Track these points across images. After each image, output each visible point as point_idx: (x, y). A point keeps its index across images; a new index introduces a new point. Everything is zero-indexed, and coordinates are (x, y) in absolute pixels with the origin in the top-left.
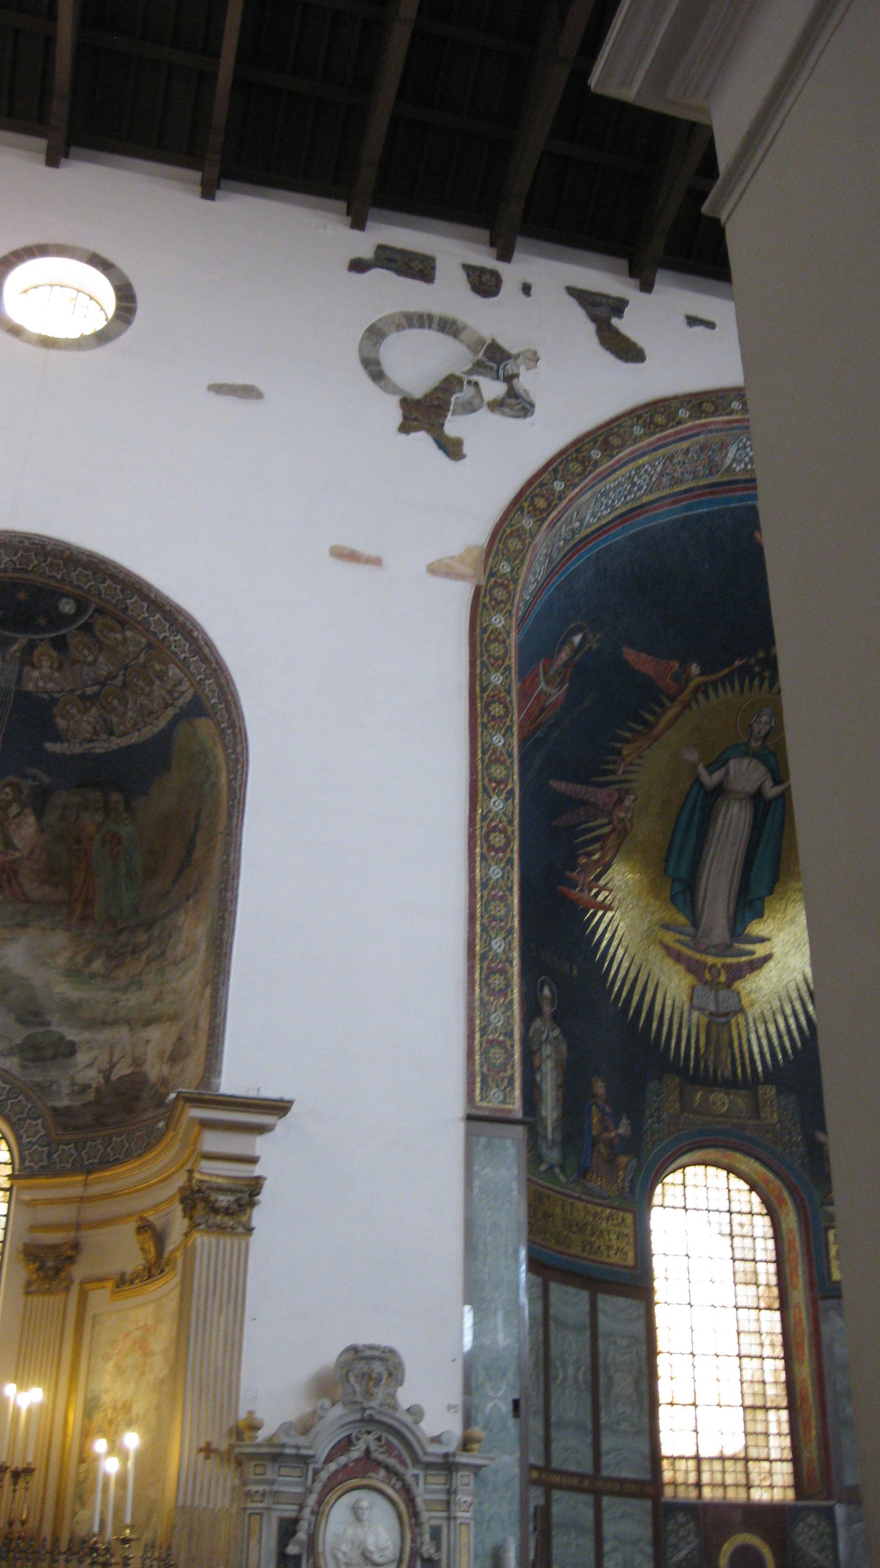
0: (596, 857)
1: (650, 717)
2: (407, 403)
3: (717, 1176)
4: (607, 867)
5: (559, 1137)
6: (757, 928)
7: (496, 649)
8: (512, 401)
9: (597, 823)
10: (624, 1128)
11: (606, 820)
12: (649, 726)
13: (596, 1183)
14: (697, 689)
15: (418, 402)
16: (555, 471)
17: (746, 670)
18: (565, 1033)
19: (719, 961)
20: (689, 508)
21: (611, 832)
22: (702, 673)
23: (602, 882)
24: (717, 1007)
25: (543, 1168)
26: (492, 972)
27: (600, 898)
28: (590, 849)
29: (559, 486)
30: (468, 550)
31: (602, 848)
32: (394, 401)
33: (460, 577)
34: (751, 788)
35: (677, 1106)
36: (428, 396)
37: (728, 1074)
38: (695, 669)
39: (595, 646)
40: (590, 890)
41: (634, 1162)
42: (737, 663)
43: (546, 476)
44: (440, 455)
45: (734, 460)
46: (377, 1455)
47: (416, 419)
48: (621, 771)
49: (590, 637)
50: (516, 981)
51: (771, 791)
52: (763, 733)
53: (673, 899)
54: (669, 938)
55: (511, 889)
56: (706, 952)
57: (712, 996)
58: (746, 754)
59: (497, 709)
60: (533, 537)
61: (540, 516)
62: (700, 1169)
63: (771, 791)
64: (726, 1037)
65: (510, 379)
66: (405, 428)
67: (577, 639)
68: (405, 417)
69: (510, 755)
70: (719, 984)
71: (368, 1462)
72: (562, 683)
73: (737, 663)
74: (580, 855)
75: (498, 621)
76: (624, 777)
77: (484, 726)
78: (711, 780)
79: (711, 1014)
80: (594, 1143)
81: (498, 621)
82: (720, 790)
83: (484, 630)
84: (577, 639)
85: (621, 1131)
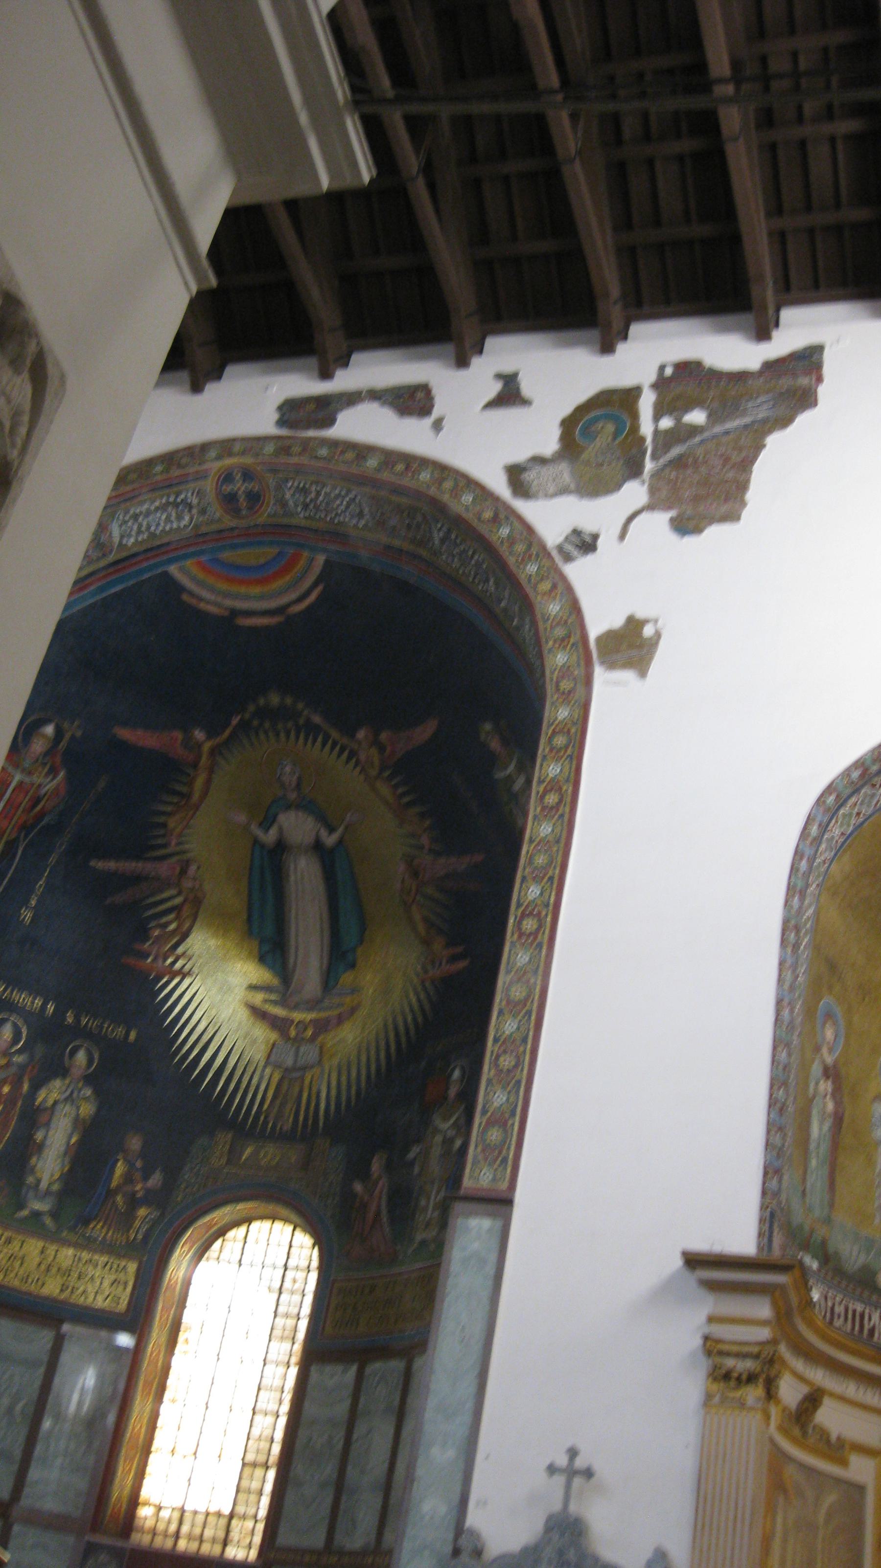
0: (173, 926)
1: (184, 789)
3: (281, 1231)
4: (185, 936)
5: (56, 1187)
6: (347, 978)
9: (165, 895)
10: (156, 1180)
11: (173, 892)
12: (188, 796)
13: (97, 1230)
14: (213, 752)
17: (244, 725)
18: (97, 1092)
19: (308, 1016)
20: (102, 589)
21: (185, 901)
22: (210, 736)
23: (180, 950)
24: (295, 1061)
25: (25, 1213)
27: (178, 965)
28: (164, 920)
31: (177, 918)
34: (309, 839)
35: (224, 1161)
37: (288, 1126)
38: (199, 735)
39: (79, 734)
40: (165, 959)
41: (156, 1214)
42: (235, 721)
45: (122, 537)
48: (173, 843)
49: (66, 725)
51: (330, 840)
52: (294, 783)
53: (262, 959)
54: (258, 998)
56: (295, 1007)
57: (292, 1053)
58: (288, 807)
62: (266, 1224)
63: (330, 840)
64: (296, 1090)
67: (49, 730)
70: (303, 1039)
72: (53, 771)
73: (235, 721)
74: (151, 928)
76: (178, 849)
78: (270, 837)
79: (286, 1070)
80: (111, 1193)
82: (281, 848)
84: (49, 730)
85: (151, 1183)
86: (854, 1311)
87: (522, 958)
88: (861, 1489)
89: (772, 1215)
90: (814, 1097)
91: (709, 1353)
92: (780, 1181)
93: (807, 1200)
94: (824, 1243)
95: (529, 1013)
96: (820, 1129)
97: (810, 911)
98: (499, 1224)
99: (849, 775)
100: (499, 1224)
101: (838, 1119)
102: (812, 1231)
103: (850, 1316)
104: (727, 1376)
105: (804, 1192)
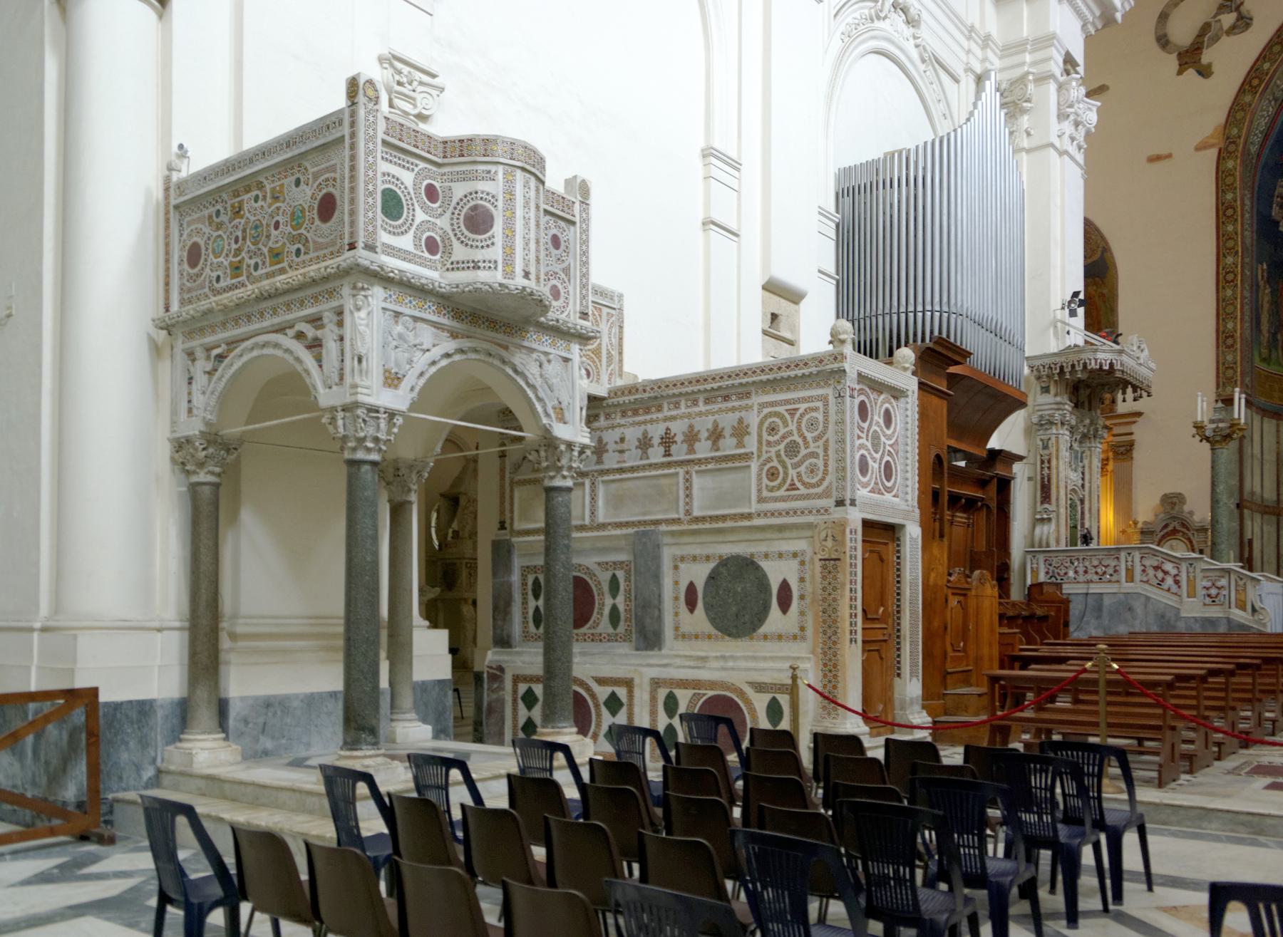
2: (1180, 56)
7: (1229, 180)
8: (1239, 23)
15: (1187, 51)
16: (1264, 57)
26: (1227, 337)
29: (1266, 66)
30: (1216, 129)
32: (1174, 56)
33: (1212, 146)
36: (1192, 44)
43: (1259, 63)
44: (1200, 79)
46: (1178, 528)
47: (1186, 63)
50: (1239, 340)
55: (1236, 299)
59: (1230, 212)
60: (1250, 105)
61: (1253, 90)
65: (1237, 9)
66: (1180, 73)
68: (1180, 65)
69: (1236, 234)
71: (1174, 531)
75: (1230, 164)
77: (1223, 223)
81: (1230, 164)
83: (1223, 172)
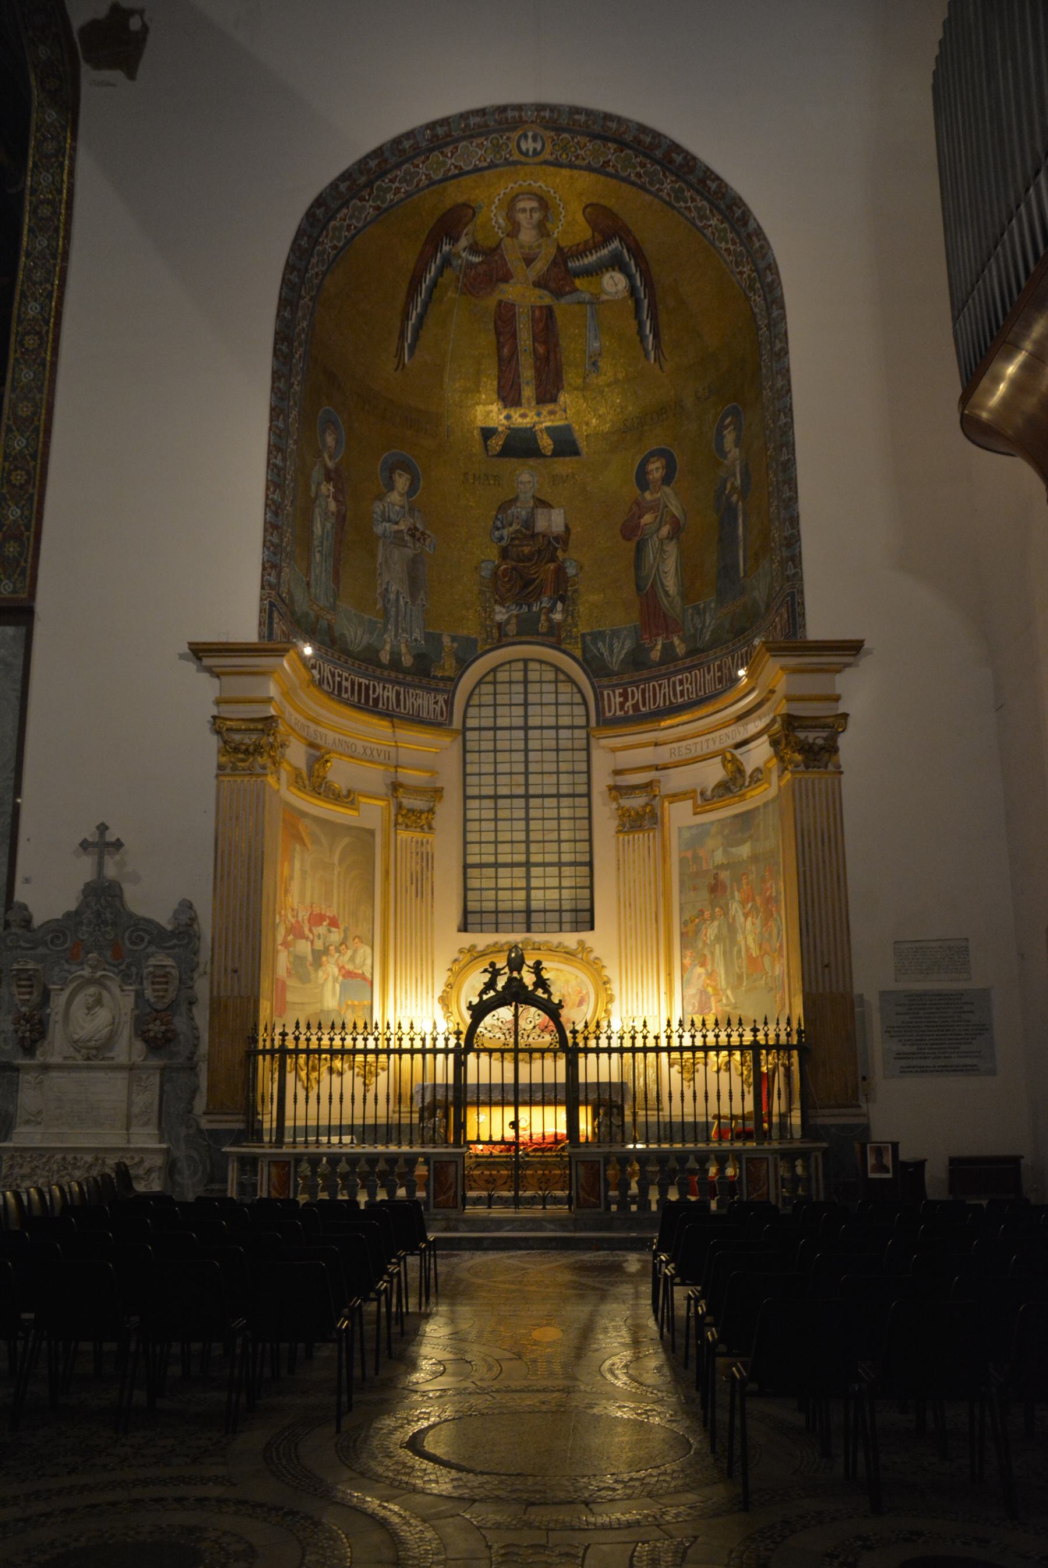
86: (360, 684)
87: (27, 376)
88: (372, 833)
89: (271, 604)
90: (317, 497)
91: (218, 732)
92: (279, 576)
93: (313, 590)
94: (330, 627)
95: (37, 430)
96: (323, 527)
97: (305, 324)
98: (23, 630)
99: (337, 186)
100: (23, 630)
101: (341, 518)
102: (318, 617)
103: (356, 687)
104: (236, 750)
105: (308, 584)
